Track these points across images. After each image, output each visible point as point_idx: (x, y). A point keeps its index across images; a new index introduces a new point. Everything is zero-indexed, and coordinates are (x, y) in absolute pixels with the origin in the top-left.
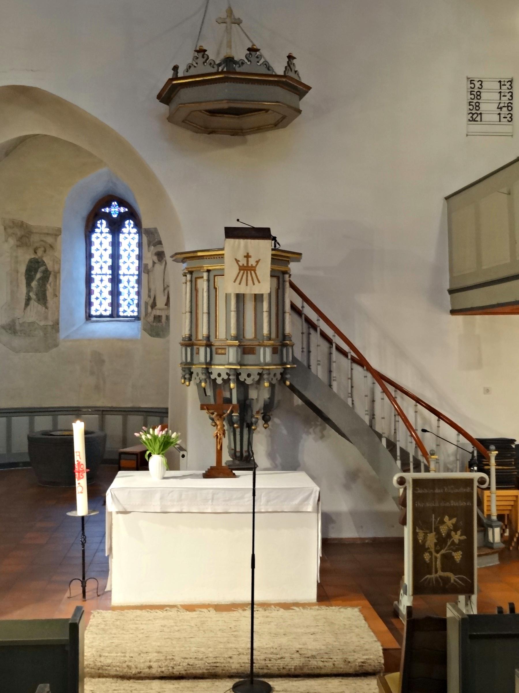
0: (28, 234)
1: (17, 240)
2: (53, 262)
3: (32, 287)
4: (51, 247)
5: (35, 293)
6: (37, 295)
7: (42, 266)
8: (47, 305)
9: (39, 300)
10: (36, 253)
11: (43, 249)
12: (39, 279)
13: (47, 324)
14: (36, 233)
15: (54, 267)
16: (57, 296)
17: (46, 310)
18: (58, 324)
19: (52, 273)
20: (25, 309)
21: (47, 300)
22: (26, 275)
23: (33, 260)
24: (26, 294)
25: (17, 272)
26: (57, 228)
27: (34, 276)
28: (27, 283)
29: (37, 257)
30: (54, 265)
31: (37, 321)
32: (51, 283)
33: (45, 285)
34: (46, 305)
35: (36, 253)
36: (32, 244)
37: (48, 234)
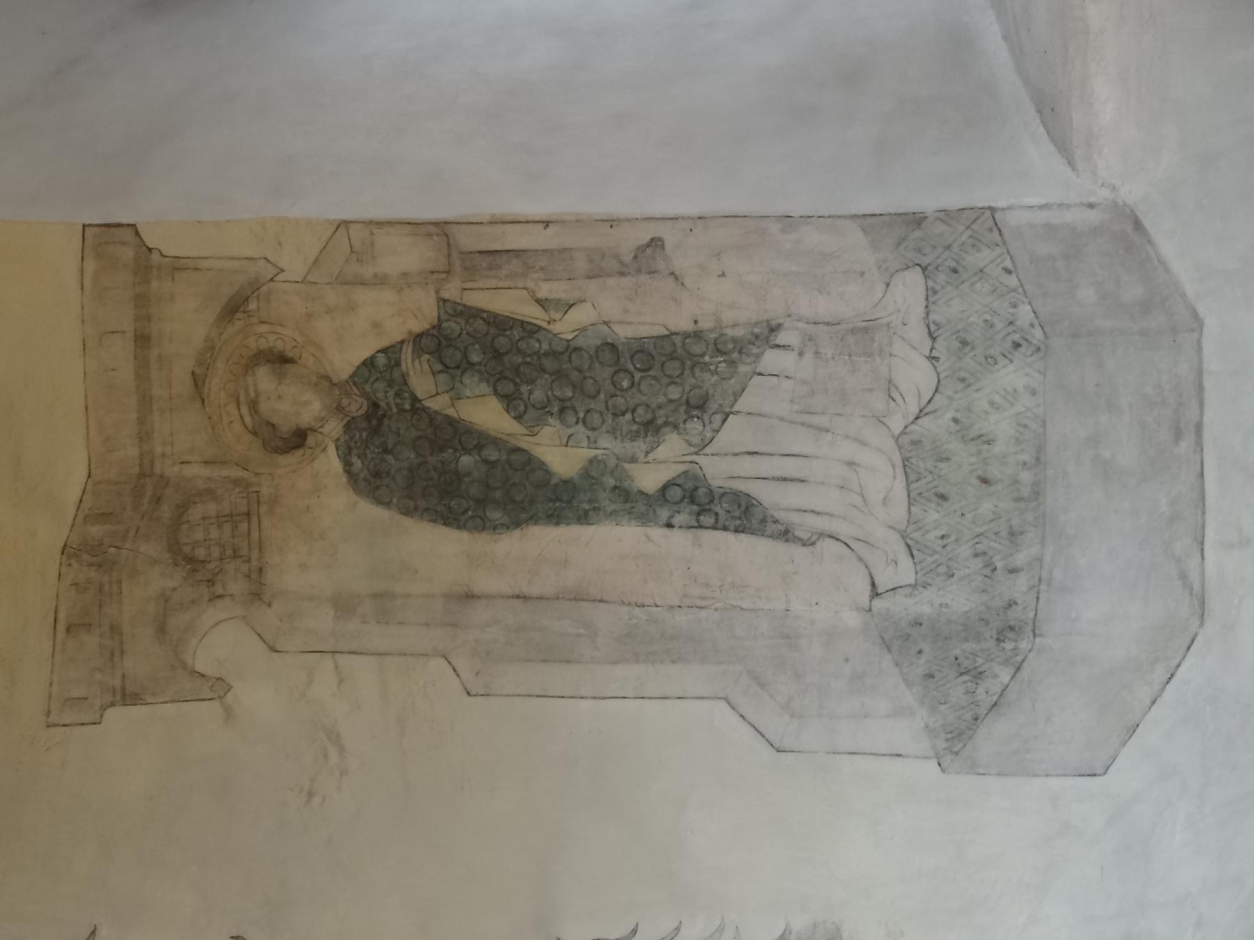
0: (158, 500)
1: (216, 597)
2: (363, 283)
3: (591, 474)
4: (234, 308)
5: (640, 446)
6: (651, 428)
7: (402, 385)
8: (739, 332)
9: (697, 406)
10: (298, 439)
11: (264, 379)
12: (509, 400)
13: (917, 333)
14: (144, 436)
15: (405, 281)
16: (656, 243)
17: (782, 338)
18: (916, 220)
19: (451, 291)
20: (786, 535)
21: (697, 335)
22: (484, 526)
23: (357, 464)
24: (644, 519)
25: (470, 597)
26: (90, 266)
27: (493, 455)
28: (555, 518)
29: (334, 427)
30: (381, 281)
31: (897, 426)
32: (542, 303)
33: (571, 349)
34: (741, 346)
35: (298, 439)
36: (236, 473)
37: (142, 340)
